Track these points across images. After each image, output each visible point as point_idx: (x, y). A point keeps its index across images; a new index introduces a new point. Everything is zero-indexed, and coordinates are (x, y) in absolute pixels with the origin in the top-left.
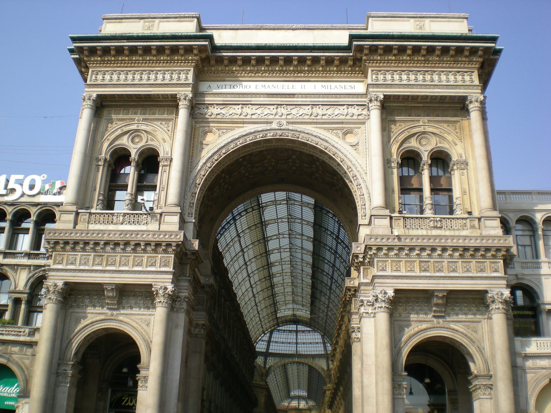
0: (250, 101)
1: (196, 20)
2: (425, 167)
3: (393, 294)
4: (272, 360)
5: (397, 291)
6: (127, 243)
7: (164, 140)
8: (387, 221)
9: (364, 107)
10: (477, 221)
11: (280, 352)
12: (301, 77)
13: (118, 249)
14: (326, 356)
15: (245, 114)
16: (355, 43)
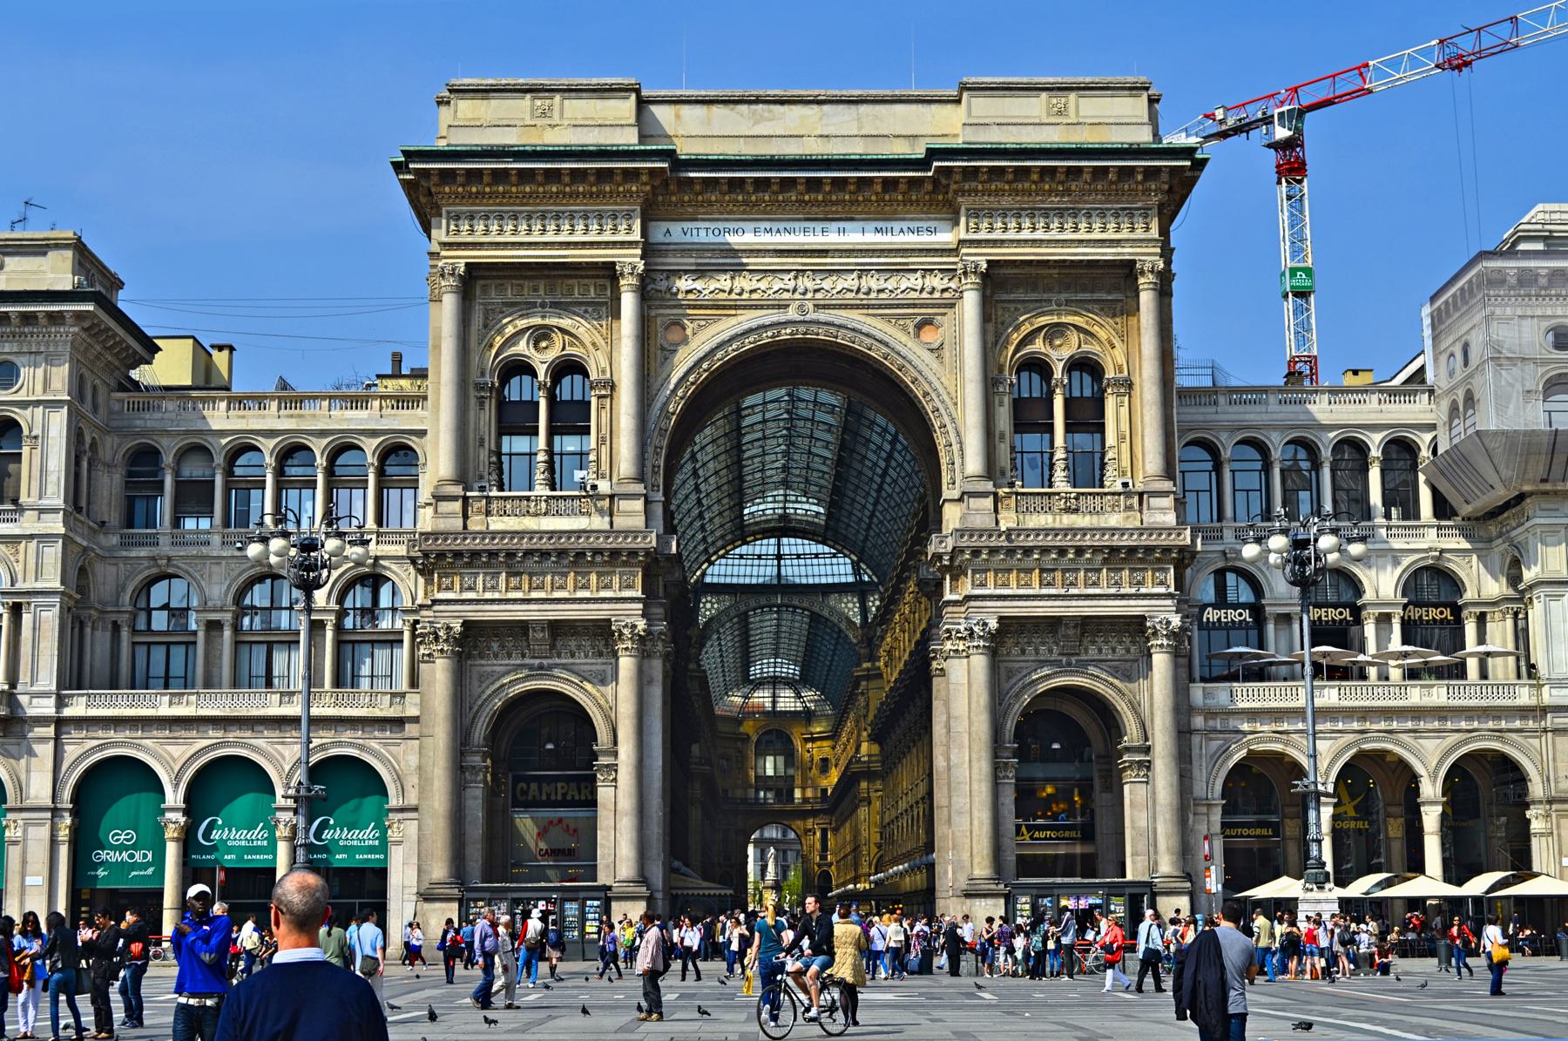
0: (747, 264)
1: (633, 96)
2: (1058, 391)
3: (996, 625)
4: (713, 604)
5: (1001, 619)
6: (562, 553)
7: (594, 344)
8: (988, 503)
9: (951, 274)
10: (1136, 499)
11: (735, 581)
12: (836, 212)
13: (548, 564)
14: (858, 589)
15: (737, 290)
16: (936, 164)
